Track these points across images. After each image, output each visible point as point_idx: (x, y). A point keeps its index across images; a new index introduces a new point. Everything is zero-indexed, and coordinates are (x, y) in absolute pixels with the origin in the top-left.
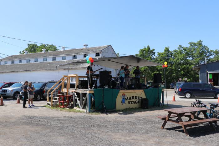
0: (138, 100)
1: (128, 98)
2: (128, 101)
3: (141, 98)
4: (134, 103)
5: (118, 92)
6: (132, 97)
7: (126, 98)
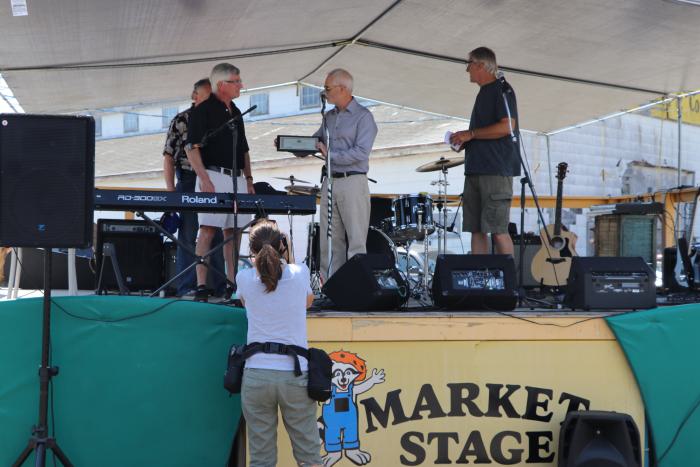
0: (525, 426)
1: (393, 398)
3: (575, 402)
4: (482, 459)
6: (455, 389)
7: (370, 405)
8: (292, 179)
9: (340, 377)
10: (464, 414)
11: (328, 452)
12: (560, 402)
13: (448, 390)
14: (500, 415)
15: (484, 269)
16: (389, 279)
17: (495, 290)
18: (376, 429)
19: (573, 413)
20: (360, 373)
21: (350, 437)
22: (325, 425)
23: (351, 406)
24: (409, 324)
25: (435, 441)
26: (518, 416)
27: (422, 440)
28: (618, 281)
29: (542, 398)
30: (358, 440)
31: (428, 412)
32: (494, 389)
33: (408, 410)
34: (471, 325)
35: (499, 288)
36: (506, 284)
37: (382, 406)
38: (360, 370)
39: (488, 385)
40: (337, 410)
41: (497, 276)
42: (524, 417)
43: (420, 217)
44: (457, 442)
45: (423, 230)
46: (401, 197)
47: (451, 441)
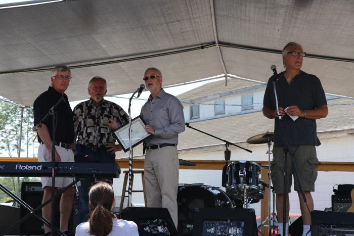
15: (227, 220)
28: (341, 232)
41: (239, 226)
43: (242, 179)
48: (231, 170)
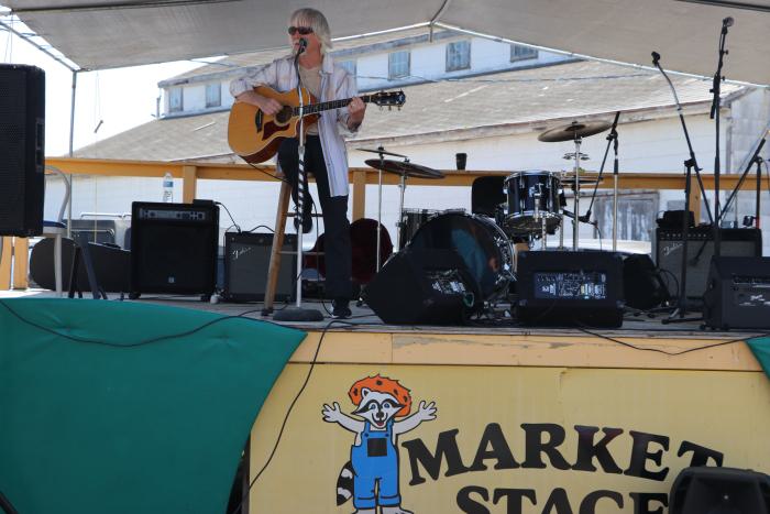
0: (629, 485)
1: (448, 441)
2: (450, 485)
3: (701, 455)
5: (283, 358)
6: (532, 431)
7: (416, 448)
8: (381, 151)
9: (376, 411)
10: (544, 466)
11: (358, 509)
12: (680, 454)
13: (523, 432)
14: (594, 469)
15: (578, 272)
16: (453, 284)
17: (592, 299)
18: (423, 480)
19: (698, 470)
20: (403, 406)
21: (387, 489)
22: (354, 473)
23: (390, 449)
24: (468, 342)
25: (504, 500)
26: (618, 471)
27: (486, 498)
29: (653, 447)
30: (399, 495)
31: (495, 461)
32: (585, 434)
33: (468, 458)
34: (554, 346)
35: (598, 297)
36: (608, 292)
37: (432, 449)
38: (403, 402)
39: (577, 428)
40: (370, 454)
41: (597, 281)
42: (627, 473)
43: (537, 201)
44: (534, 503)
45: (540, 220)
46: (515, 175)
47: (525, 500)
48: (488, 188)
